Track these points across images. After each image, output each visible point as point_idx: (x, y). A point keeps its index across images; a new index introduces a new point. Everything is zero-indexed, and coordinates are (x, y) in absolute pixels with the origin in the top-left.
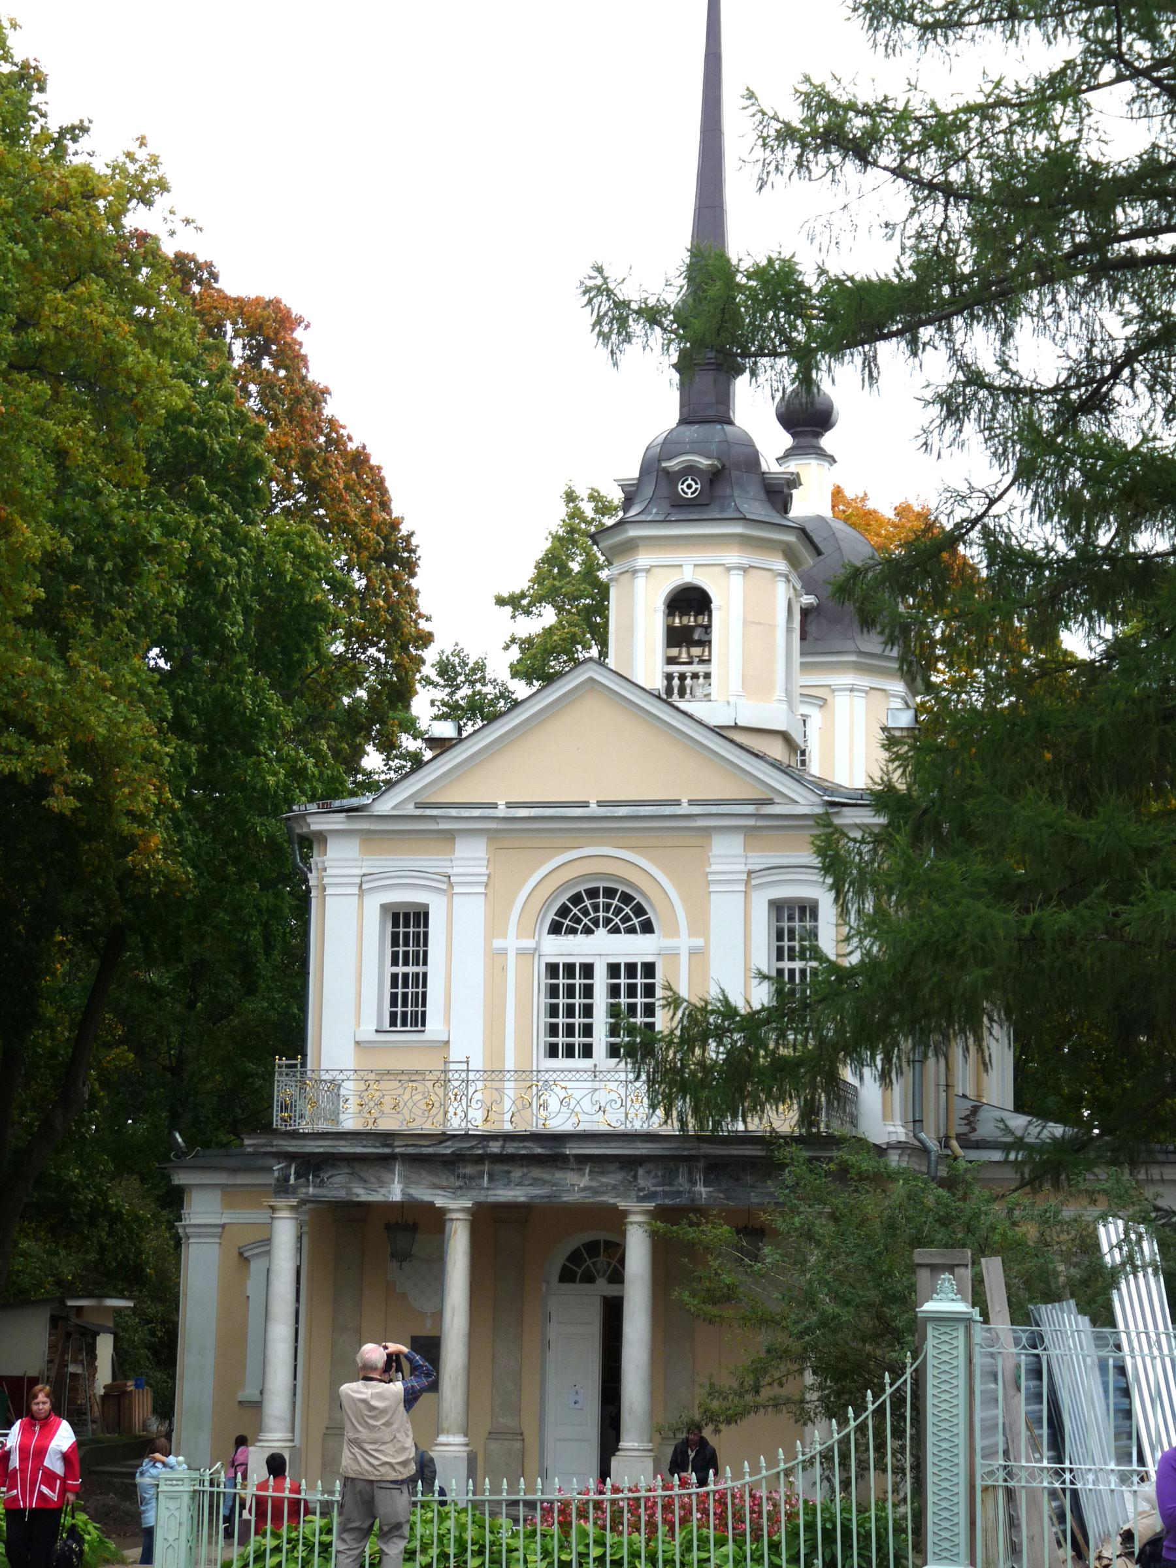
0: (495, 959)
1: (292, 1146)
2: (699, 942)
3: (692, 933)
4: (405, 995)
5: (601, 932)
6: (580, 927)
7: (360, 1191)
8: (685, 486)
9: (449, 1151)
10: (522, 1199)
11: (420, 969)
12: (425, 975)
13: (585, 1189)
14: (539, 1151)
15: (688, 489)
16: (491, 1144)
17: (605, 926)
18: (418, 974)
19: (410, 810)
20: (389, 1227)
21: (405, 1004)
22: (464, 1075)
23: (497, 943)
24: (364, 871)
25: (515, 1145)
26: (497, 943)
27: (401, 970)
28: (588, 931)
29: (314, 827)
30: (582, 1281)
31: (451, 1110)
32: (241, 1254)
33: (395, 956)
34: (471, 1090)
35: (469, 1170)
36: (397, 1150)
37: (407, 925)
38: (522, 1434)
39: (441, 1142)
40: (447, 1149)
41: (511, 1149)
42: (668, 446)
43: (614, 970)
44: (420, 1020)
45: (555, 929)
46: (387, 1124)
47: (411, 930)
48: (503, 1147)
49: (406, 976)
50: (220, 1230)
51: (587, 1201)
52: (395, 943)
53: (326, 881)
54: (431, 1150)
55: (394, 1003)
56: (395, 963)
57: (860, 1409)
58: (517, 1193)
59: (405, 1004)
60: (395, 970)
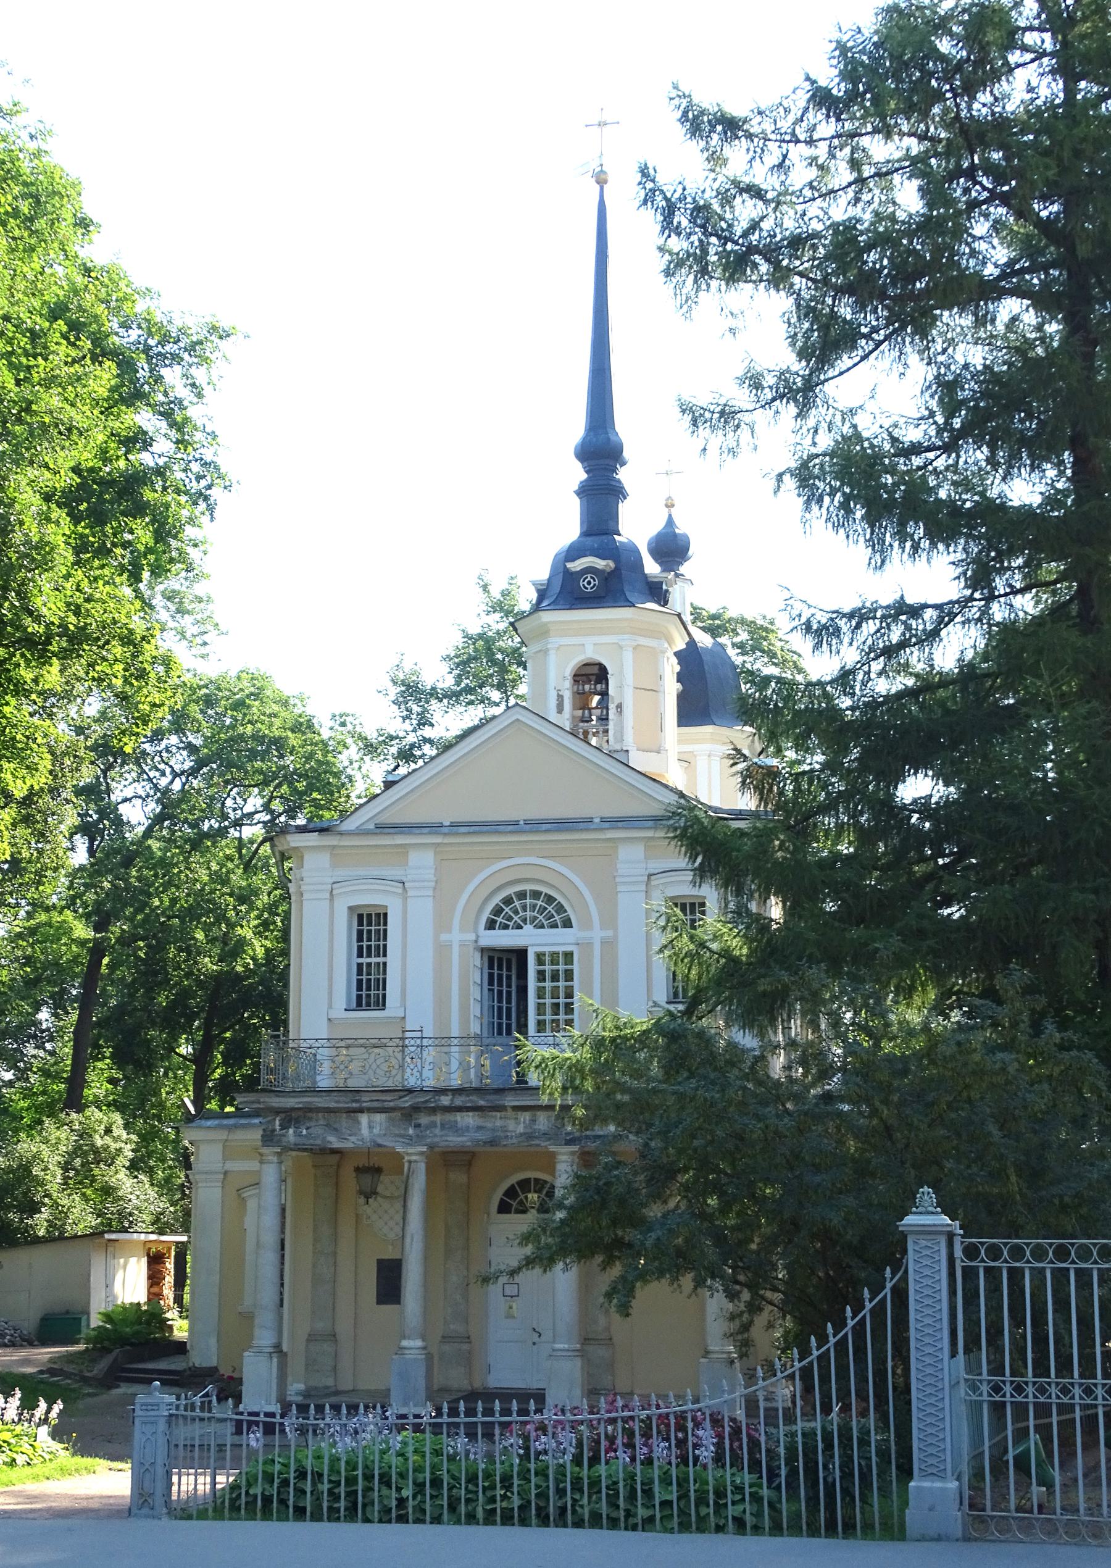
0: (442, 950)
1: (276, 1102)
2: (610, 933)
3: (603, 927)
4: (369, 981)
5: (528, 928)
6: (511, 924)
9: (407, 1105)
10: (469, 1144)
11: (381, 960)
12: (385, 964)
13: (521, 1135)
14: (482, 1103)
15: (588, 584)
16: (442, 1098)
18: (379, 964)
19: (372, 826)
20: (358, 1170)
21: (369, 989)
22: (419, 1042)
23: (444, 937)
24: (334, 880)
26: (444, 937)
27: (364, 960)
28: (520, 927)
29: (293, 845)
30: (518, 1212)
31: (408, 1070)
32: (239, 1195)
33: (360, 948)
34: (425, 1053)
35: (424, 1120)
36: (365, 1105)
37: (370, 924)
38: (469, 1338)
39: (401, 1097)
40: (407, 1102)
41: (459, 1101)
42: (573, 552)
43: (540, 958)
44: (380, 1003)
45: (491, 925)
46: (354, 1083)
47: (373, 928)
48: (452, 1100)
49: (369, 965)
52: (360, 939)
53: (304, 888)
54: (392, 1104)
55: (359, 988)
56: (360, 955)
57: (840, 1324)
58: (464, 1139)
59: (369, 989)
60: (360, 960)
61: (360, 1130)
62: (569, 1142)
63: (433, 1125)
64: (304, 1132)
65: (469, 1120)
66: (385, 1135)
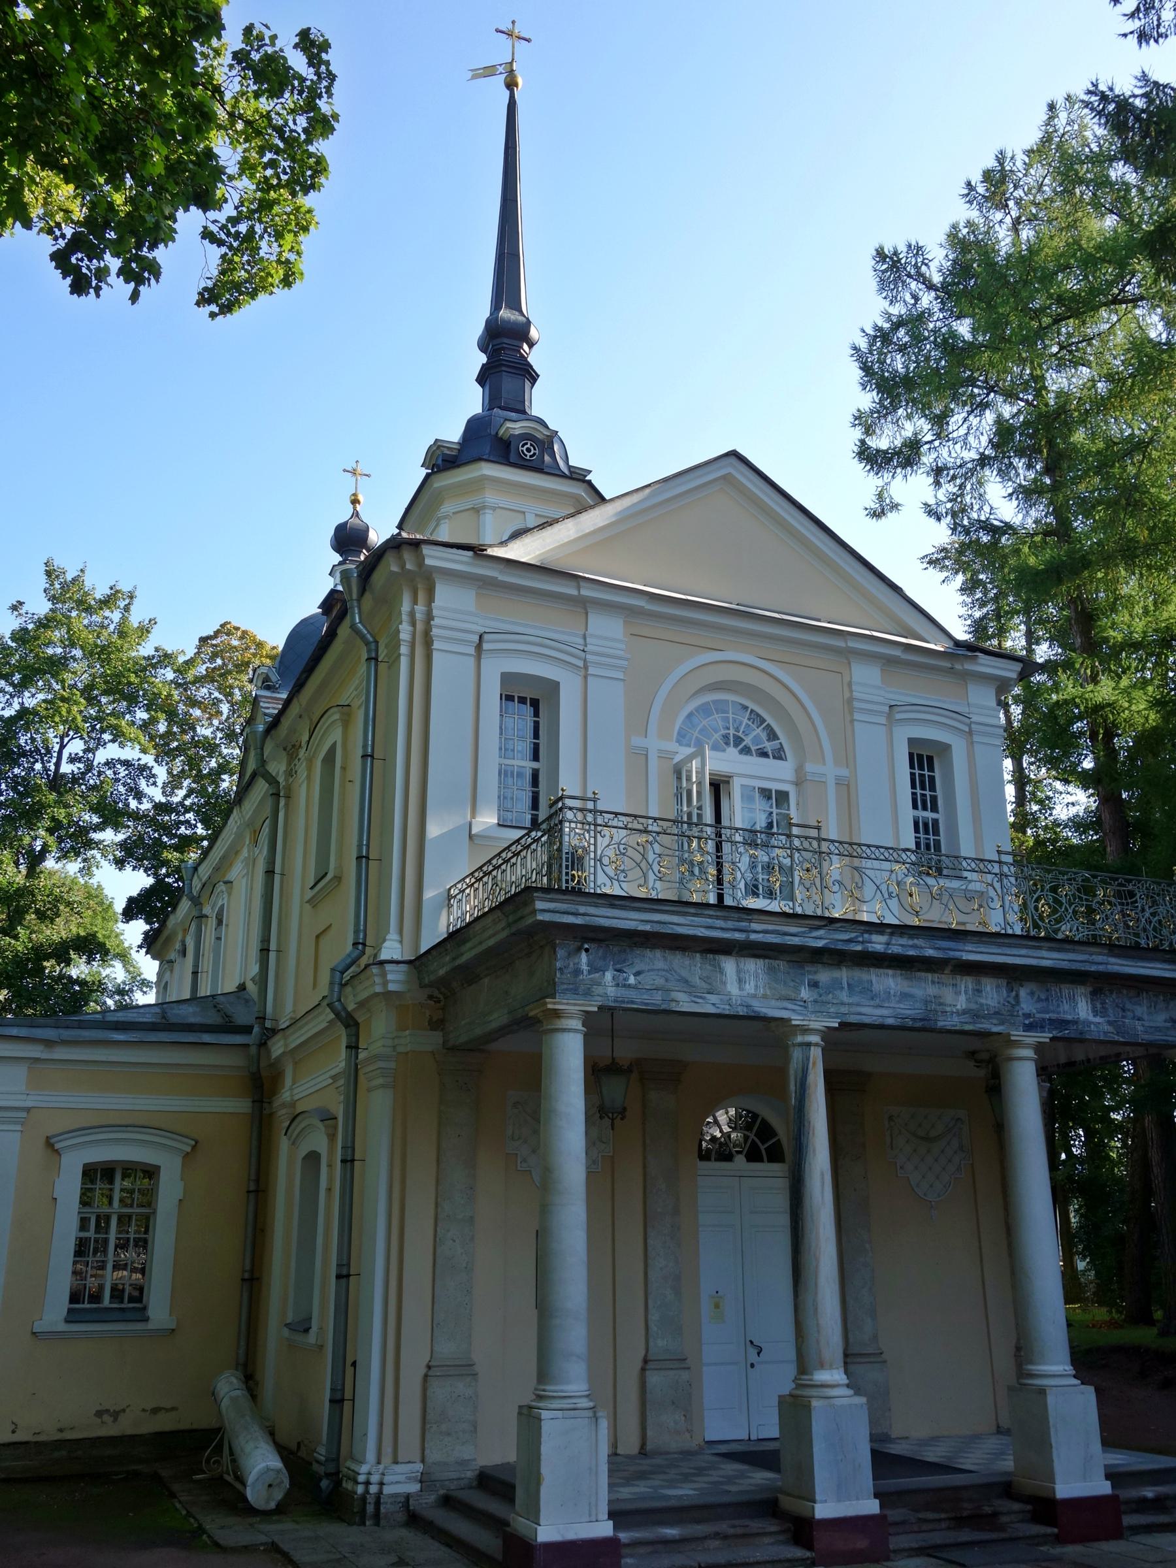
2: (844, 772)
5: (732, 751)
7: (681, 996)
8: (524, 449)
9: (820, 944)
10: (890, 1021)
13: (964, 1012)
14: (930, 952)
17: (736, 745)
25: (904, 941)
26: (637, 741)
29: (428, 562)
36: (753, 937)
40: (819, 939)
50: (24, 1115)
51: (968, 1027)
54: (796, 941)
58: (885, 1012)
61: (725, 983)
62: (1029, 1028)
63: (836, 985)
64: (632, 980)
65: (887, 982)
66: (765, 996)
